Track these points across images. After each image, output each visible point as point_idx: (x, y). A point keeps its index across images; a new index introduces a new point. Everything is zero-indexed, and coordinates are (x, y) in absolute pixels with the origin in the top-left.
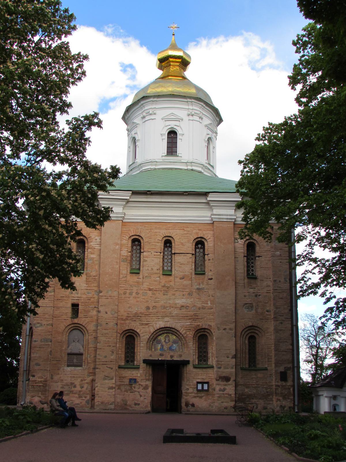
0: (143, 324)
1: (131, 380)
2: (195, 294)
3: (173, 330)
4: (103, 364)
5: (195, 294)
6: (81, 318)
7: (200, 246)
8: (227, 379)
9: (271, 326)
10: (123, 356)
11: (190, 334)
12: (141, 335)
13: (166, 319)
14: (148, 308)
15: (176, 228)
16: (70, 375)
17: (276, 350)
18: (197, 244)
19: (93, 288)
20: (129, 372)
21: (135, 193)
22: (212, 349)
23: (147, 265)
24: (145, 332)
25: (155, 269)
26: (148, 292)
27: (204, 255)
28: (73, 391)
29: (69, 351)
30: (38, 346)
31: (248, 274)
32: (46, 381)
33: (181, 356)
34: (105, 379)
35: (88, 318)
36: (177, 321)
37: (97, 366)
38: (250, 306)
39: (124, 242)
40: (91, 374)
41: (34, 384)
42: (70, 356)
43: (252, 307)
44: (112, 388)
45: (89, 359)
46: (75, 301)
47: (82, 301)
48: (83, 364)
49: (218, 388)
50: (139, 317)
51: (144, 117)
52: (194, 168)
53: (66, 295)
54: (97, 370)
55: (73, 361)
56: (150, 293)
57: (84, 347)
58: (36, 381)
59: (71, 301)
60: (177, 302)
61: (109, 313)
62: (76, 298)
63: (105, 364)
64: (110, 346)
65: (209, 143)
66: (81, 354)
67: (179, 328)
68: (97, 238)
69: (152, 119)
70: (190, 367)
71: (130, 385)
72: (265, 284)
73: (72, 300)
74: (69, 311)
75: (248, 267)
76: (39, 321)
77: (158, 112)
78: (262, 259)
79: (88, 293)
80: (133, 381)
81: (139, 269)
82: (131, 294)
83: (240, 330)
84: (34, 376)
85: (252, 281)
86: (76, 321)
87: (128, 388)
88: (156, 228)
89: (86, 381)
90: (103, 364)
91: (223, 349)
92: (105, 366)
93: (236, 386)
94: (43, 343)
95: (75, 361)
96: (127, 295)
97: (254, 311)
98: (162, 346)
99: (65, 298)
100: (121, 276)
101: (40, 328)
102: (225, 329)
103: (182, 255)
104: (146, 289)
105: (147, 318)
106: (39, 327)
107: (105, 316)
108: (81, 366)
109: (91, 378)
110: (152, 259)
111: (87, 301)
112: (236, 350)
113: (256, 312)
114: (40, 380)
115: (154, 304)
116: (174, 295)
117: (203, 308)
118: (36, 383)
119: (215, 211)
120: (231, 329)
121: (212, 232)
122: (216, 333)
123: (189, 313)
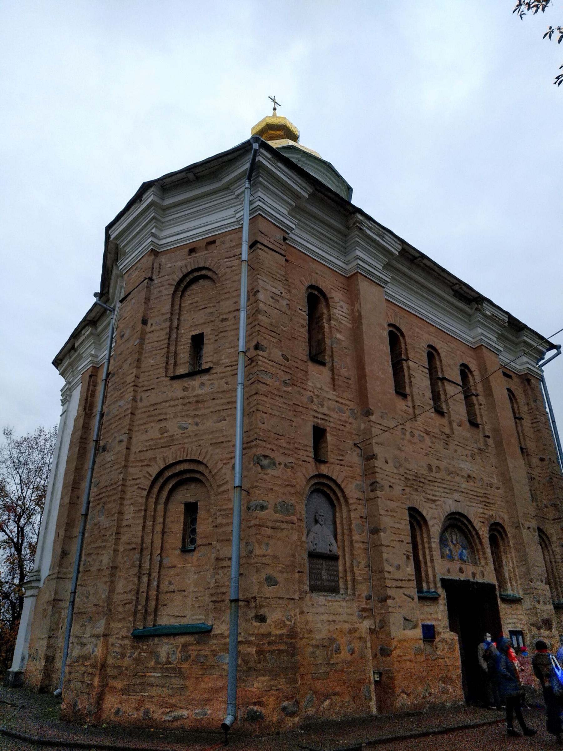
0: (428, 499)
2: (478, 458)
4: (397, 587)
5: (478, 458)
6: (333, 464)
12: (430, 523)
13: (456, 496)
15: (439, 338)
16: (325, 617)
19: (347, 402)
23: (418, 386)
24: (435, 518)
26: (425, 435)
30: (269, 524)
35: (346, 468)
36: (469, 503)
37: (390, 592)
40: (364, 614)
42: (315, 561)
46: (320, 421)
48: (342, 585)
50: (421, 485)
53: (301, 402)
54: (389, 602)
55: (320, 574)
56: (427, 438)
57: (339, 537)
59: (312, 419)
60: (462, 466)
62: (320, 416)
63: (401, 587)
64: (402, 541)
68: (342, 303)
73: (314, 417)
74: (310, 442)
76: (268, 453)
79: (341, 411)
84: (262, 619)
89: (357, 635)
90: (397, 587)
92: (402, 591)
94: (279, 516)
99: (300, 409)
101: (270, 471)
103: (453, 385)
104: (422, 430)
105: (433, 488)
107: (385, 467)
109: (367, 624)
111: (341, 428)
114: (278, 632)
115: (437, 463)
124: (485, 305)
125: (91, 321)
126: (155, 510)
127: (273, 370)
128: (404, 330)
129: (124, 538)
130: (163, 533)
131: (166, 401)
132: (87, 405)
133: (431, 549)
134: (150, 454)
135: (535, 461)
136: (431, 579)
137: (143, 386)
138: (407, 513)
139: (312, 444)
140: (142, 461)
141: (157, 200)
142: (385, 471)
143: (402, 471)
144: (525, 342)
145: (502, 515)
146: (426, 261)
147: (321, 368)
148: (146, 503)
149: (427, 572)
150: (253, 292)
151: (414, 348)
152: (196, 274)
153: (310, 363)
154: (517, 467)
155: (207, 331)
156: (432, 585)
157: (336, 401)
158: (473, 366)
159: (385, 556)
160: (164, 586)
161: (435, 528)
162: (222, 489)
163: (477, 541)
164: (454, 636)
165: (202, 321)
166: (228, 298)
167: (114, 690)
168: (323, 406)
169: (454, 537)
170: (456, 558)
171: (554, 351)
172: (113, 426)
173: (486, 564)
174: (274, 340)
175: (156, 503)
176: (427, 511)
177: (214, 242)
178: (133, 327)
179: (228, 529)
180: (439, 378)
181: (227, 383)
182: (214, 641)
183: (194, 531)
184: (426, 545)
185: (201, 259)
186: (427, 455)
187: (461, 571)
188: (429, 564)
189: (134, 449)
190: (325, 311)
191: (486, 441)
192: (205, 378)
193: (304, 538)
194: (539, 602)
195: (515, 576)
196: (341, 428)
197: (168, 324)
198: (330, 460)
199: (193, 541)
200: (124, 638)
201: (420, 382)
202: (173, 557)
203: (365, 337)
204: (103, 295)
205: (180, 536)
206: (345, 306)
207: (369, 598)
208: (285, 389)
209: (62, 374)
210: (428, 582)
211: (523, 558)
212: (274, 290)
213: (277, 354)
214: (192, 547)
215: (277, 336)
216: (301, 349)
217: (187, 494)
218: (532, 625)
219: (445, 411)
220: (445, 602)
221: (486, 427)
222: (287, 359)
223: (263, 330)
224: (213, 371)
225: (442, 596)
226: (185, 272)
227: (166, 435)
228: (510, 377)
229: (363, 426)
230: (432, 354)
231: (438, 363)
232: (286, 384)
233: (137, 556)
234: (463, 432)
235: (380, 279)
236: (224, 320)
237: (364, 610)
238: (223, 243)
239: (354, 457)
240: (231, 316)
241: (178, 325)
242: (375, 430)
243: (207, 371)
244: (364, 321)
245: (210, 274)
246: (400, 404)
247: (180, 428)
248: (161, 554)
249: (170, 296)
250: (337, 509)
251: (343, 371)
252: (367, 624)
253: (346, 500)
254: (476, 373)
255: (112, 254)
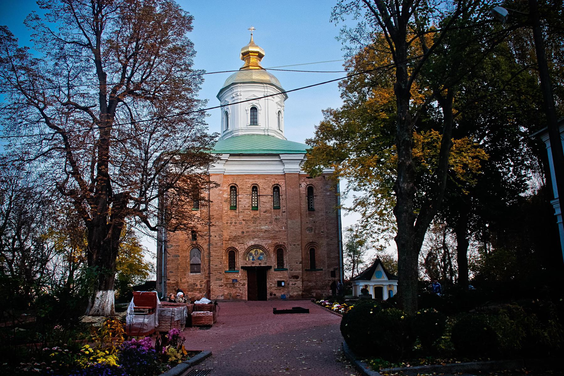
1: (233, 280)
7: (276, 190)
8: (296, 277)
9: (324, 242)
10: (228, 264)
11: (272, 249)
13: (256, 239)
14: (243, 232)
17: (329, 257)
18: (274, 188)
21: (231, 155)
22: (286, 259)
25: (247, 206)
27: (279, 196)
29: (192, 263)
31: (309, 208)
32: (177, 282)
33: (266, 263)
34: (216, 280)
38: (310, 229)
39: (225, 188)
43: (312, 230)
44: (222, 286)
49: (291, 283)
52: (269, 133)
56: (244, 222)
61: (217, 237)
65: (279, 115)
66: (200, 264)
70: (272, 270)
71: (234, 284)
72: (320, 214)
75: (308, 203)
78: (318, 198)
80: (235, 281)
81: (236, 206)
82: (231, 223)
83: (304, 245)
84: (169, 280)
85: (312, 212)
87: (232, 285)
88: (246, 179)
91: (294, 258)
93: (302, 282)
95: (195, 269)
96: (229, 224)
97: (313, 232)
98: (253, 257)
100: (224, 212)
107: (215, 239)
108: (200, 272)
110: (244, 200)
112: (302, 258)
113: (315, 232)
117: (280, 231)
119: (287, 166)
120: (298, 245)
121: (284, 180)
122: (289, 248)
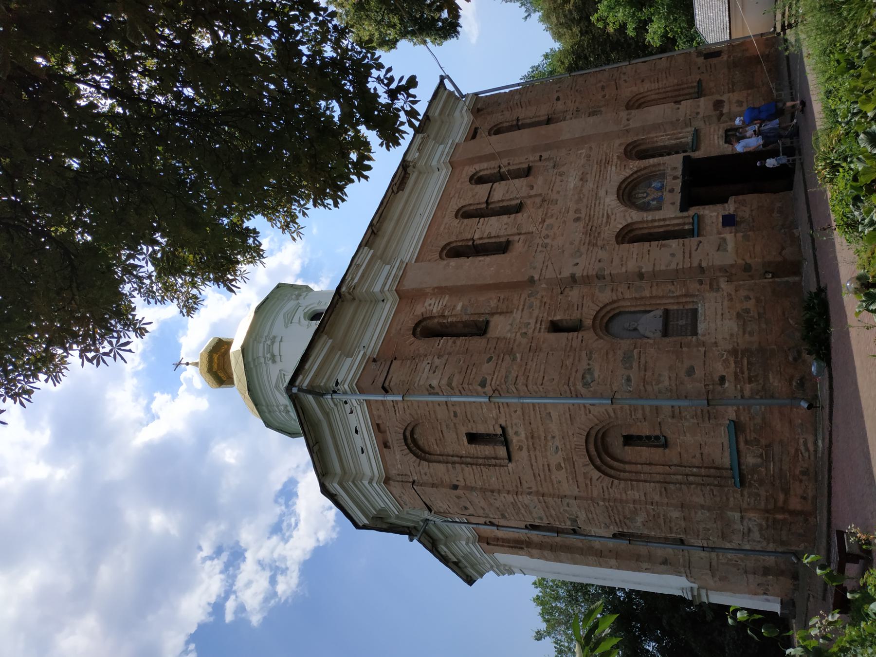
2: (562, 169)
3: (624, 186)
4: (690, 257)
5: (562, 169)
6: (582, 314)
12: (630, 221)
13: (602, 193)
16: (719, 323)
20: (708, 228)
24: (625, 216)
28: (759, 314)
29: (659, 334)
30: (642, 373)
35: (585, 302)
37: (695, 264)
41: (746, 375)
45: (678, 293)
46: (543, 327)
47: (545, 314)
48: (690, 306)
50: (594, 229)
51: (273, 357)
54: (704, 265)
55: (681, 326)
56: (548, 222)
57: (648, 308)
58: (736, 373)
60: (572, 186)
61: (576, 261)
62: (538, 325)
63: (690, 254)
67: (622, 177)
68: (426, 304)
69: (281, 341)
70: (697, 155)
73: (540, 332)
76: (579, 375)
77: (274, 333)
79: (531, 307)
84: (722, 379)
86: (588, 322)
89: (733, 293)
90: (690, 257)
92: (693, 253)
94: (635, 365)
95: (682, 322)
99: (533, 345)
101: (596, 375)
102: (628, 120)
105: (596, 218)
106: (592, 374)
108: (695, 312)
109: (723, 285)
111: (547, 306)
114: (733, 365)
115: (571, 212)
116: (558, 192)
118: (743, 373)
123: (595, 169)
124: (409, 158)
125: (433, 545)
126: (630, 472)
127: (503, 371)
128: (444, 243)
129: (657, 498)
130: (650, 464)
131: (532, 466)
132: (517, 546)
133: (653, 221)
134: (581, 479)
135: (560, 106)
136: (680, 221)
137: (517, 486)
138: (622, 246)
139: (566, 334)
140: (586, 485)
141: (337, 479)
142: (585, 265)
143: (583, 249)
144: (441, 113)
145: (617, 147)
146: (375, 222)
147: (492, 324)
148: (625, 480)
149: (674, 225)
150: (431, 390)
151: (460, 233)
152: (409, 441)
153: (488, 336)
154: (570, 129)
155: (463, 430)
156: (687, 220)
157: (523, 310)
158: (470, 170)
159: (663, 268)
160: (697, 462)
161: (634, 216)
162: (612, 414)
163: (643, 172)
164: (732, 200)
165: (455, 436)
166: (434, 411)
167: (786, 501)
168: (529, 324)
169: (640, 195)
170: (660, 194)
171: (446, 81)
172: (553, 512)
173: (664, 164)
174: (474, 370)
175: (624, 471)
176: (619, 224)
177: (378, 425)
178: (459, 497)
179: (647, 410)
180: (487, 208)
181: (515, 412)
182: (742, 418)
183: (648, 438)
184: (650, 225)
185: (395, 438)
186: (564, 222)
187: (672, 191)
188: (668, 223)
189: (576, 492)
190: (436, 320)
191: (545, 159)
192: (510, 432)
193: (651, 341)
194: (698, 113)
195: (674, 134)
196: (547, 306)
197: (457, 466)
198: (579, 316)
199: (657, 438)
200: (742, 495)
201: (493, 228)
202: (671, 455)
203: (459, 284)
204: (410, 532)
205: (653, 450)
206: (428, 301)
207: (701, 282)
208: (519, 360)
209: (481, 576)
210: (684, 224)
211: (656, 127)
212: (427, 370)
213: (487, 368)
214: (663, 439)
215: (470, 367)
216: (477, 343)
217: (616, 444)
218: (719, 120)
219: (519, 201)
220: (701, 207)
221: (531, 159)
222: (490, 359)
223: (466, 380)
224: (503, 424)
225: (696, 211)
226: (407, 451)
227: (563, 465)
228: (476, 129)
229: (544, 286)
230: (465, 214)
231: (472, 208)
232: (514, 359)
233: (672, 486)
234: (539, 183)
235: (399, 268)
236: (455, 415)
237: (711, 285)
238: (379, 417)
239: (574, 294)
240: (452, 409)
241: (458, 456)
242: (549, 274)
243: (503, 429)
244: (443, 285)
245: (410, 428)
246: (518, 247)
247: (556, 453)
248: (669, 466)
249: (431, 464)
250: (622, 310)
251: (493, 303)
252: (723, 285)
253: (614, 302)
254: (477, 167)
255: (381, 523)
